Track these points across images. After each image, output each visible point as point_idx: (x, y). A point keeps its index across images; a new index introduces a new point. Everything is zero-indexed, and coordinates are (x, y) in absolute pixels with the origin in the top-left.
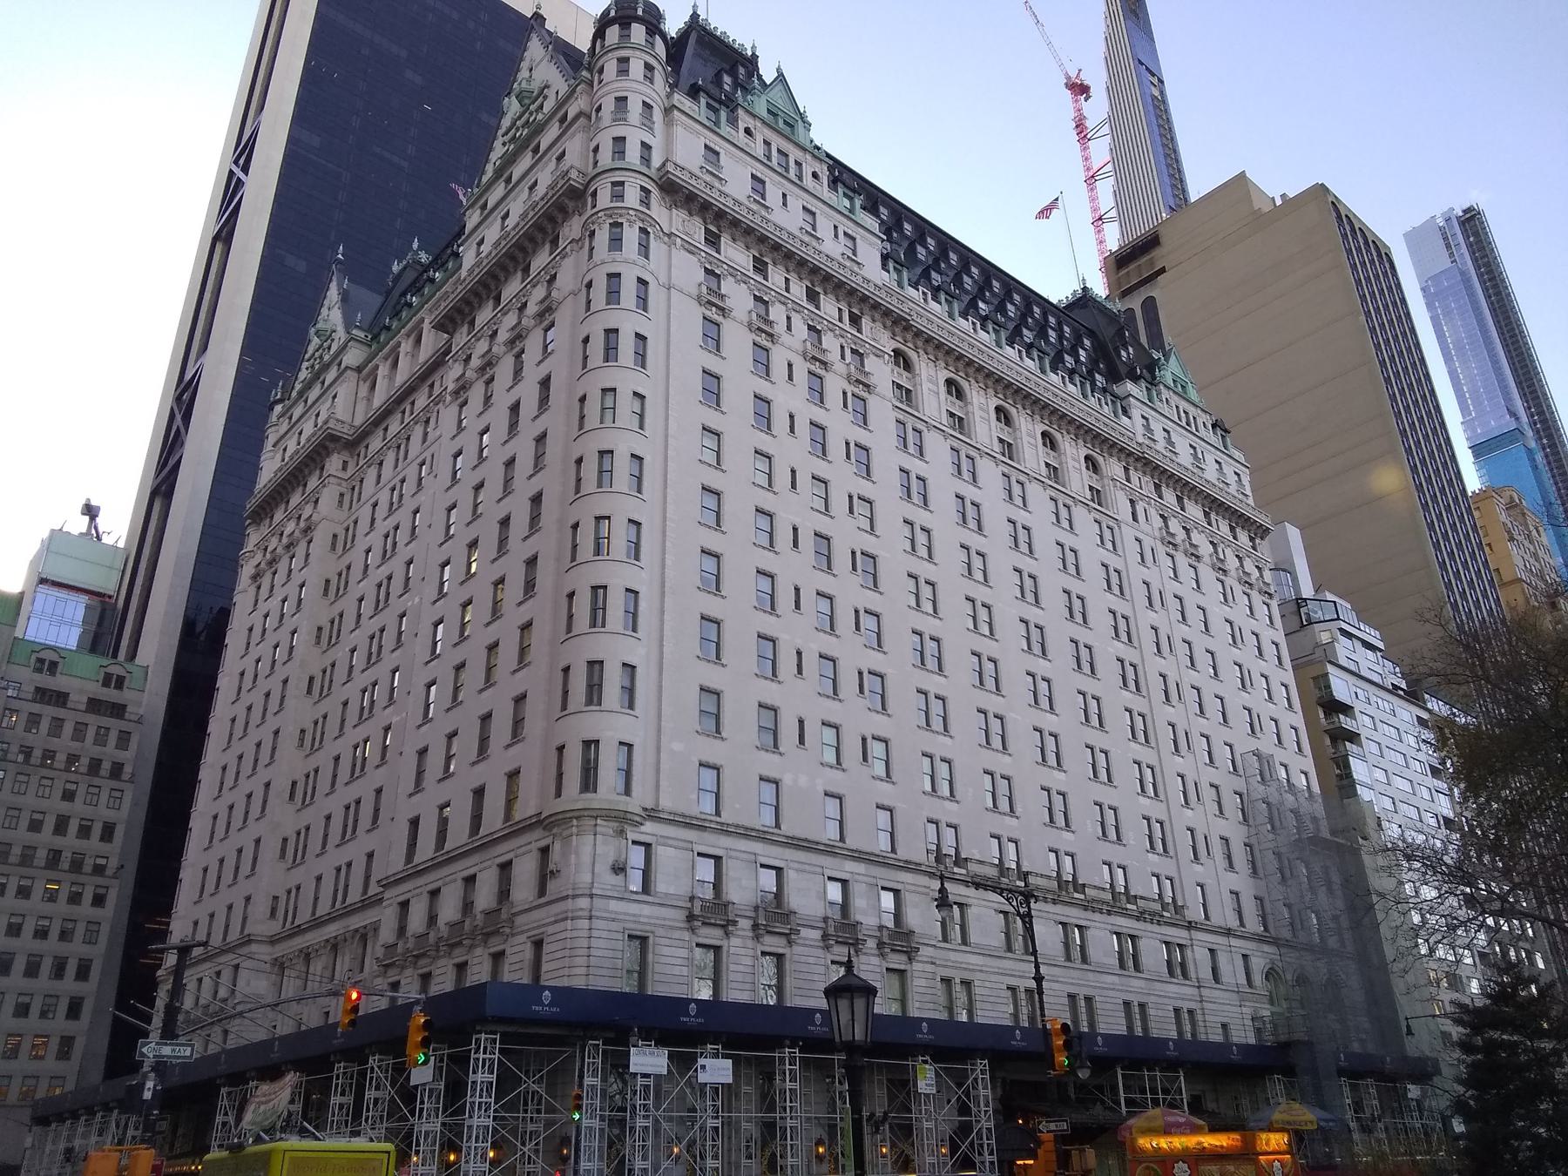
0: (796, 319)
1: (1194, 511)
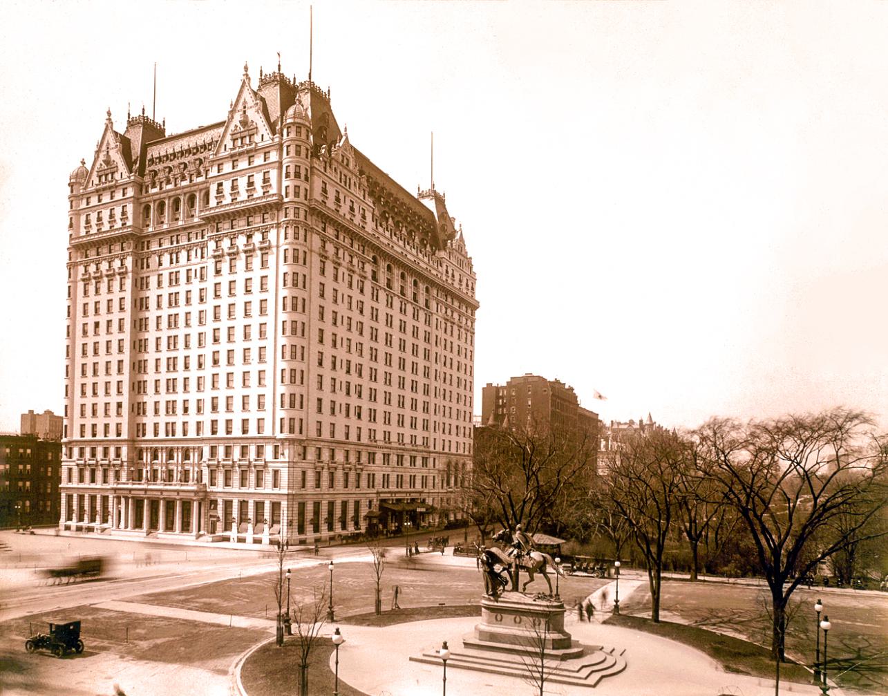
0: (346, 252)
1: (456, 304)
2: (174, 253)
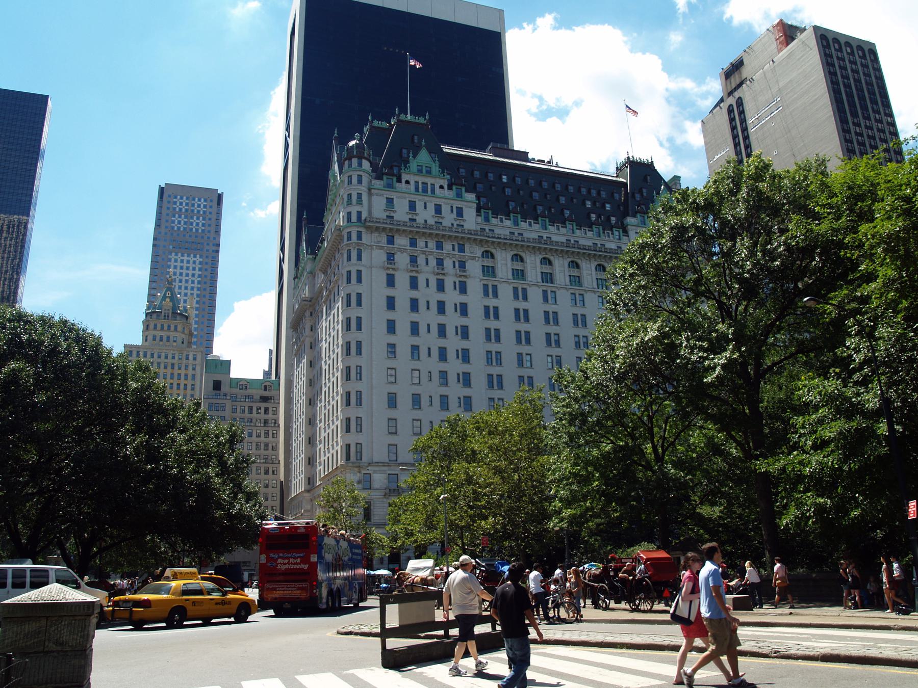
0: (430, 258)
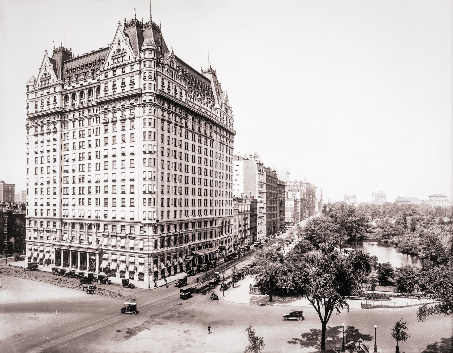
2: (81, 120)
